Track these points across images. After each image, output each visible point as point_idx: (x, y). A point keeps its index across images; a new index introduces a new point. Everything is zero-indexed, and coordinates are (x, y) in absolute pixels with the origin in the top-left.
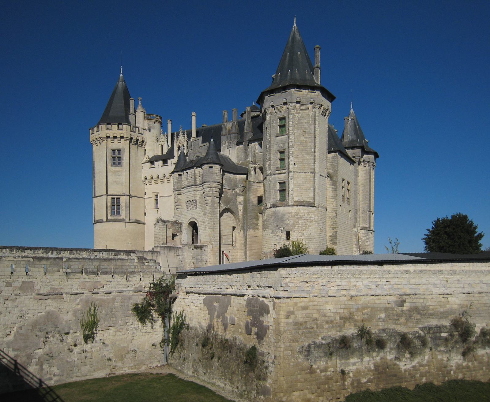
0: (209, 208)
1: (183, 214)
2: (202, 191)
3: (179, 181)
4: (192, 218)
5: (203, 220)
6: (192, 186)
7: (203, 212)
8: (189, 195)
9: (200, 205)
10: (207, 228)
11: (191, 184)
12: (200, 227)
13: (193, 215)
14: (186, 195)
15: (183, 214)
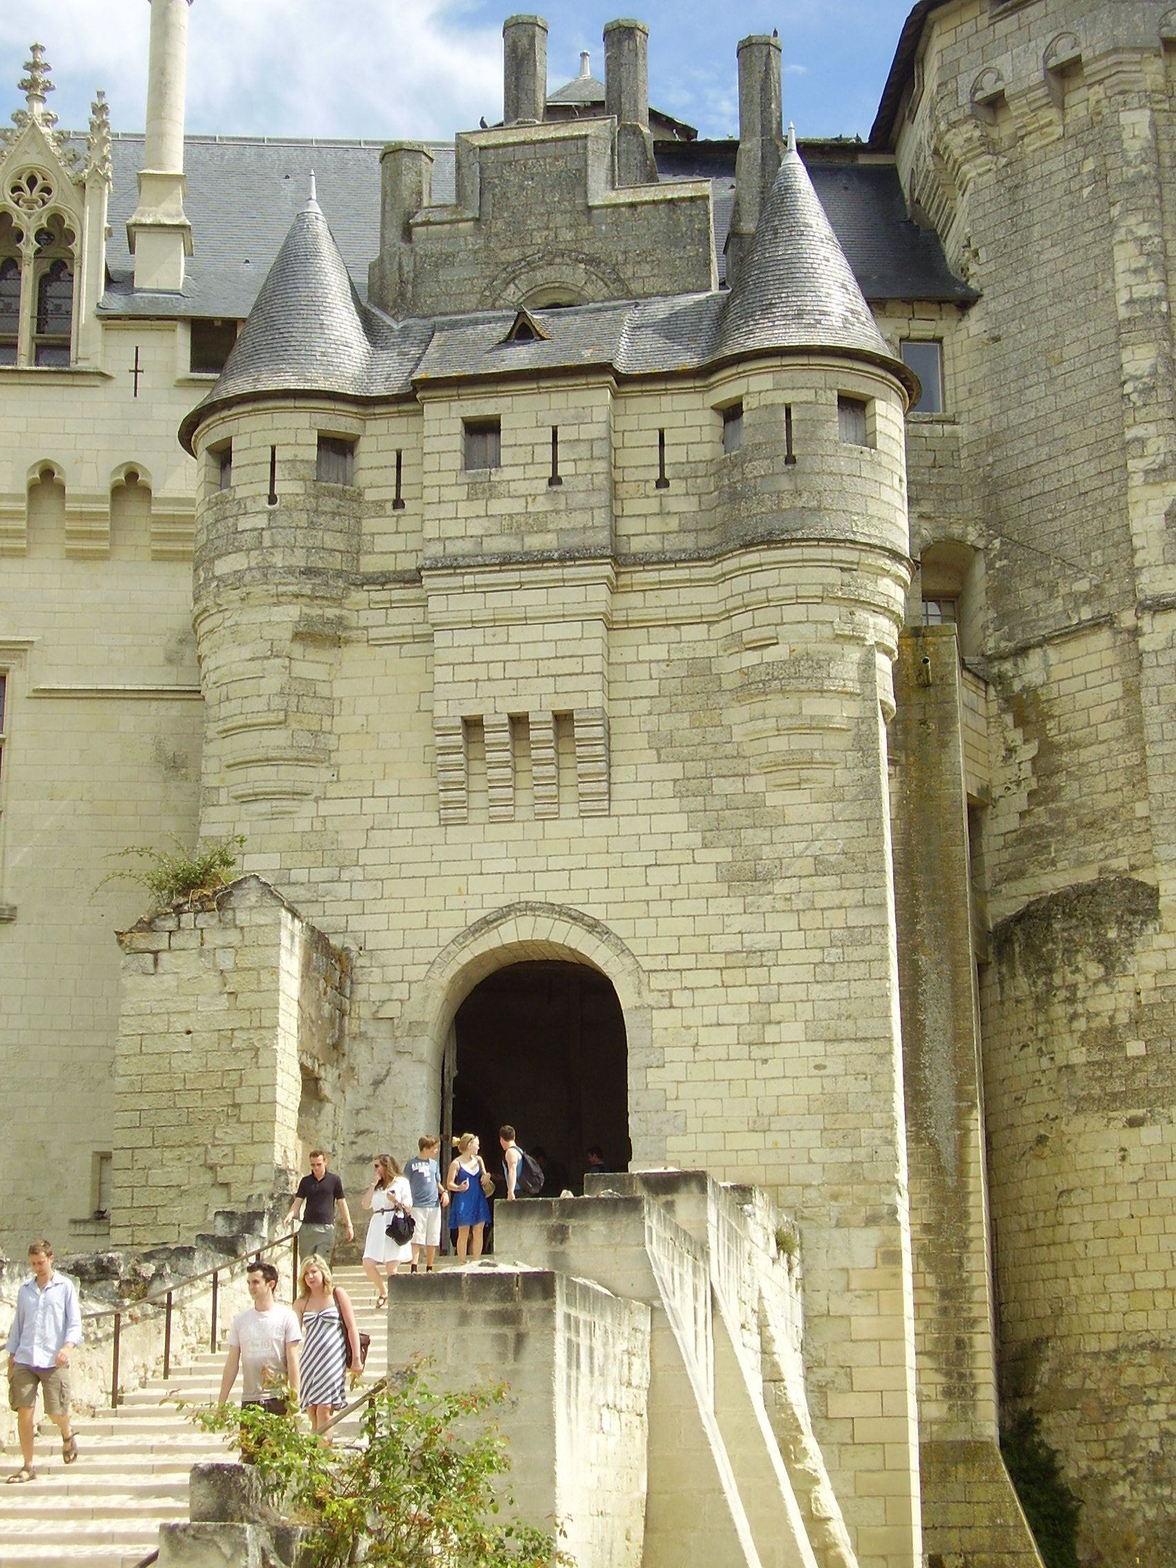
0: (819, 811)
1: (366, 857)
2: (700, 632)
3: (329, 504)
4: (530, 908)
5: (733, 943)
6: (562, 559)
7: (724, 855)
8: (510, 652)
9: (676, 770)
10: (794, 1030)
11: (535, 542)
12: (661, 1019)
13: (560, 880)
14: (452, 656)
15: (366, 857)
